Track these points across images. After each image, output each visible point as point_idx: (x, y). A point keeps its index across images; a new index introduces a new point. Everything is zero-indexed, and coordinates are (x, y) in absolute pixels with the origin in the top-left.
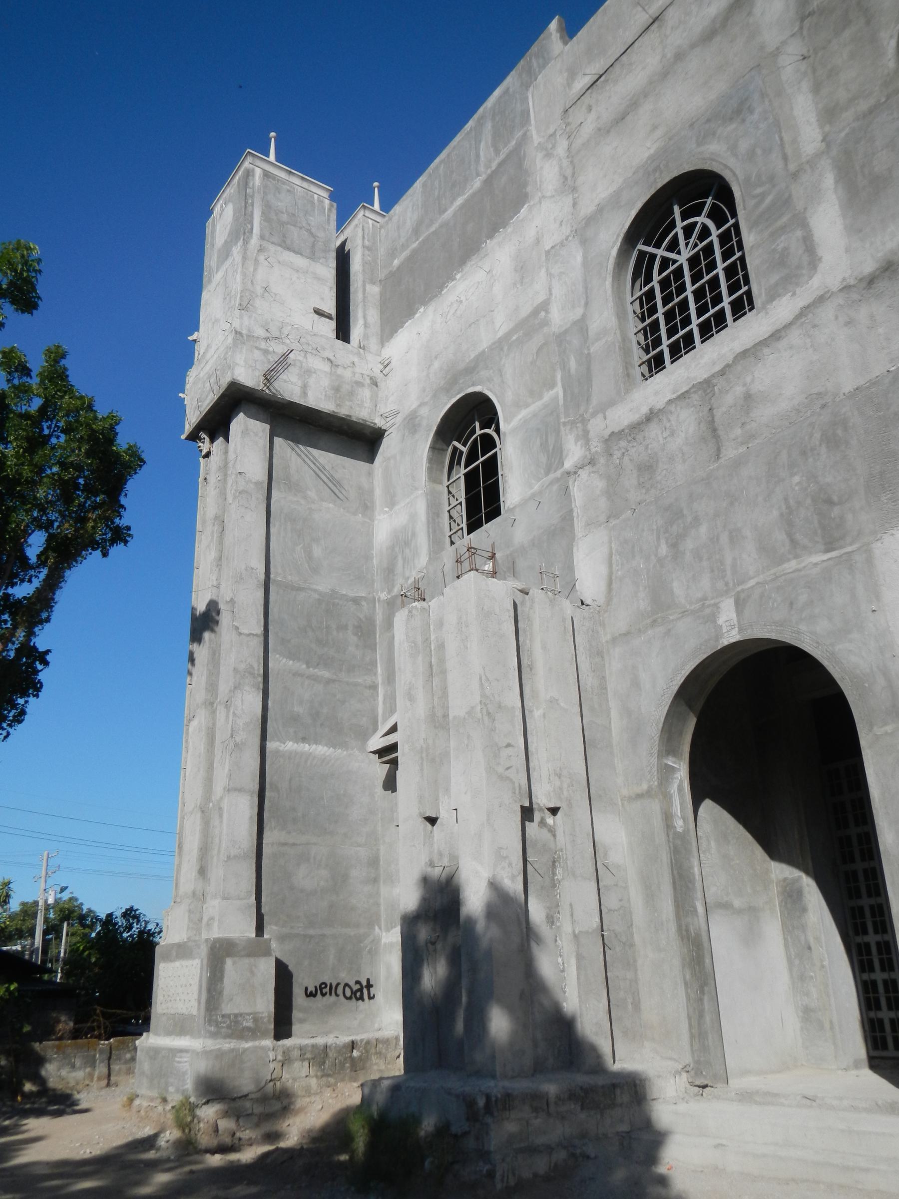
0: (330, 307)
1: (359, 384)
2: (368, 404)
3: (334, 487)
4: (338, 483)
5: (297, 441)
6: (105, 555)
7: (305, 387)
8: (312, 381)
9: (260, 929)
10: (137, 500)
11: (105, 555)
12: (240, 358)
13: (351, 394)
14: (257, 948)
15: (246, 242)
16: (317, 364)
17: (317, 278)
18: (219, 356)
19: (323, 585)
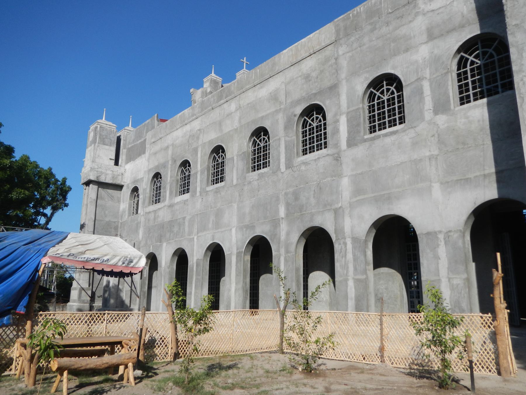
0: (113, 157)
1: (119, 175)
2: (120, 180)
3: (112, 197)
4: (113, 197)
5: (104, 188)
6: (63, 210)
7: (106, 178)
8: (107, 177)
10: (70, 197)
11: (63, 210)
12: (91, 174)
13: (116, 178)
15: (95, 145)
16: (109, 172)
19: (107, 219)
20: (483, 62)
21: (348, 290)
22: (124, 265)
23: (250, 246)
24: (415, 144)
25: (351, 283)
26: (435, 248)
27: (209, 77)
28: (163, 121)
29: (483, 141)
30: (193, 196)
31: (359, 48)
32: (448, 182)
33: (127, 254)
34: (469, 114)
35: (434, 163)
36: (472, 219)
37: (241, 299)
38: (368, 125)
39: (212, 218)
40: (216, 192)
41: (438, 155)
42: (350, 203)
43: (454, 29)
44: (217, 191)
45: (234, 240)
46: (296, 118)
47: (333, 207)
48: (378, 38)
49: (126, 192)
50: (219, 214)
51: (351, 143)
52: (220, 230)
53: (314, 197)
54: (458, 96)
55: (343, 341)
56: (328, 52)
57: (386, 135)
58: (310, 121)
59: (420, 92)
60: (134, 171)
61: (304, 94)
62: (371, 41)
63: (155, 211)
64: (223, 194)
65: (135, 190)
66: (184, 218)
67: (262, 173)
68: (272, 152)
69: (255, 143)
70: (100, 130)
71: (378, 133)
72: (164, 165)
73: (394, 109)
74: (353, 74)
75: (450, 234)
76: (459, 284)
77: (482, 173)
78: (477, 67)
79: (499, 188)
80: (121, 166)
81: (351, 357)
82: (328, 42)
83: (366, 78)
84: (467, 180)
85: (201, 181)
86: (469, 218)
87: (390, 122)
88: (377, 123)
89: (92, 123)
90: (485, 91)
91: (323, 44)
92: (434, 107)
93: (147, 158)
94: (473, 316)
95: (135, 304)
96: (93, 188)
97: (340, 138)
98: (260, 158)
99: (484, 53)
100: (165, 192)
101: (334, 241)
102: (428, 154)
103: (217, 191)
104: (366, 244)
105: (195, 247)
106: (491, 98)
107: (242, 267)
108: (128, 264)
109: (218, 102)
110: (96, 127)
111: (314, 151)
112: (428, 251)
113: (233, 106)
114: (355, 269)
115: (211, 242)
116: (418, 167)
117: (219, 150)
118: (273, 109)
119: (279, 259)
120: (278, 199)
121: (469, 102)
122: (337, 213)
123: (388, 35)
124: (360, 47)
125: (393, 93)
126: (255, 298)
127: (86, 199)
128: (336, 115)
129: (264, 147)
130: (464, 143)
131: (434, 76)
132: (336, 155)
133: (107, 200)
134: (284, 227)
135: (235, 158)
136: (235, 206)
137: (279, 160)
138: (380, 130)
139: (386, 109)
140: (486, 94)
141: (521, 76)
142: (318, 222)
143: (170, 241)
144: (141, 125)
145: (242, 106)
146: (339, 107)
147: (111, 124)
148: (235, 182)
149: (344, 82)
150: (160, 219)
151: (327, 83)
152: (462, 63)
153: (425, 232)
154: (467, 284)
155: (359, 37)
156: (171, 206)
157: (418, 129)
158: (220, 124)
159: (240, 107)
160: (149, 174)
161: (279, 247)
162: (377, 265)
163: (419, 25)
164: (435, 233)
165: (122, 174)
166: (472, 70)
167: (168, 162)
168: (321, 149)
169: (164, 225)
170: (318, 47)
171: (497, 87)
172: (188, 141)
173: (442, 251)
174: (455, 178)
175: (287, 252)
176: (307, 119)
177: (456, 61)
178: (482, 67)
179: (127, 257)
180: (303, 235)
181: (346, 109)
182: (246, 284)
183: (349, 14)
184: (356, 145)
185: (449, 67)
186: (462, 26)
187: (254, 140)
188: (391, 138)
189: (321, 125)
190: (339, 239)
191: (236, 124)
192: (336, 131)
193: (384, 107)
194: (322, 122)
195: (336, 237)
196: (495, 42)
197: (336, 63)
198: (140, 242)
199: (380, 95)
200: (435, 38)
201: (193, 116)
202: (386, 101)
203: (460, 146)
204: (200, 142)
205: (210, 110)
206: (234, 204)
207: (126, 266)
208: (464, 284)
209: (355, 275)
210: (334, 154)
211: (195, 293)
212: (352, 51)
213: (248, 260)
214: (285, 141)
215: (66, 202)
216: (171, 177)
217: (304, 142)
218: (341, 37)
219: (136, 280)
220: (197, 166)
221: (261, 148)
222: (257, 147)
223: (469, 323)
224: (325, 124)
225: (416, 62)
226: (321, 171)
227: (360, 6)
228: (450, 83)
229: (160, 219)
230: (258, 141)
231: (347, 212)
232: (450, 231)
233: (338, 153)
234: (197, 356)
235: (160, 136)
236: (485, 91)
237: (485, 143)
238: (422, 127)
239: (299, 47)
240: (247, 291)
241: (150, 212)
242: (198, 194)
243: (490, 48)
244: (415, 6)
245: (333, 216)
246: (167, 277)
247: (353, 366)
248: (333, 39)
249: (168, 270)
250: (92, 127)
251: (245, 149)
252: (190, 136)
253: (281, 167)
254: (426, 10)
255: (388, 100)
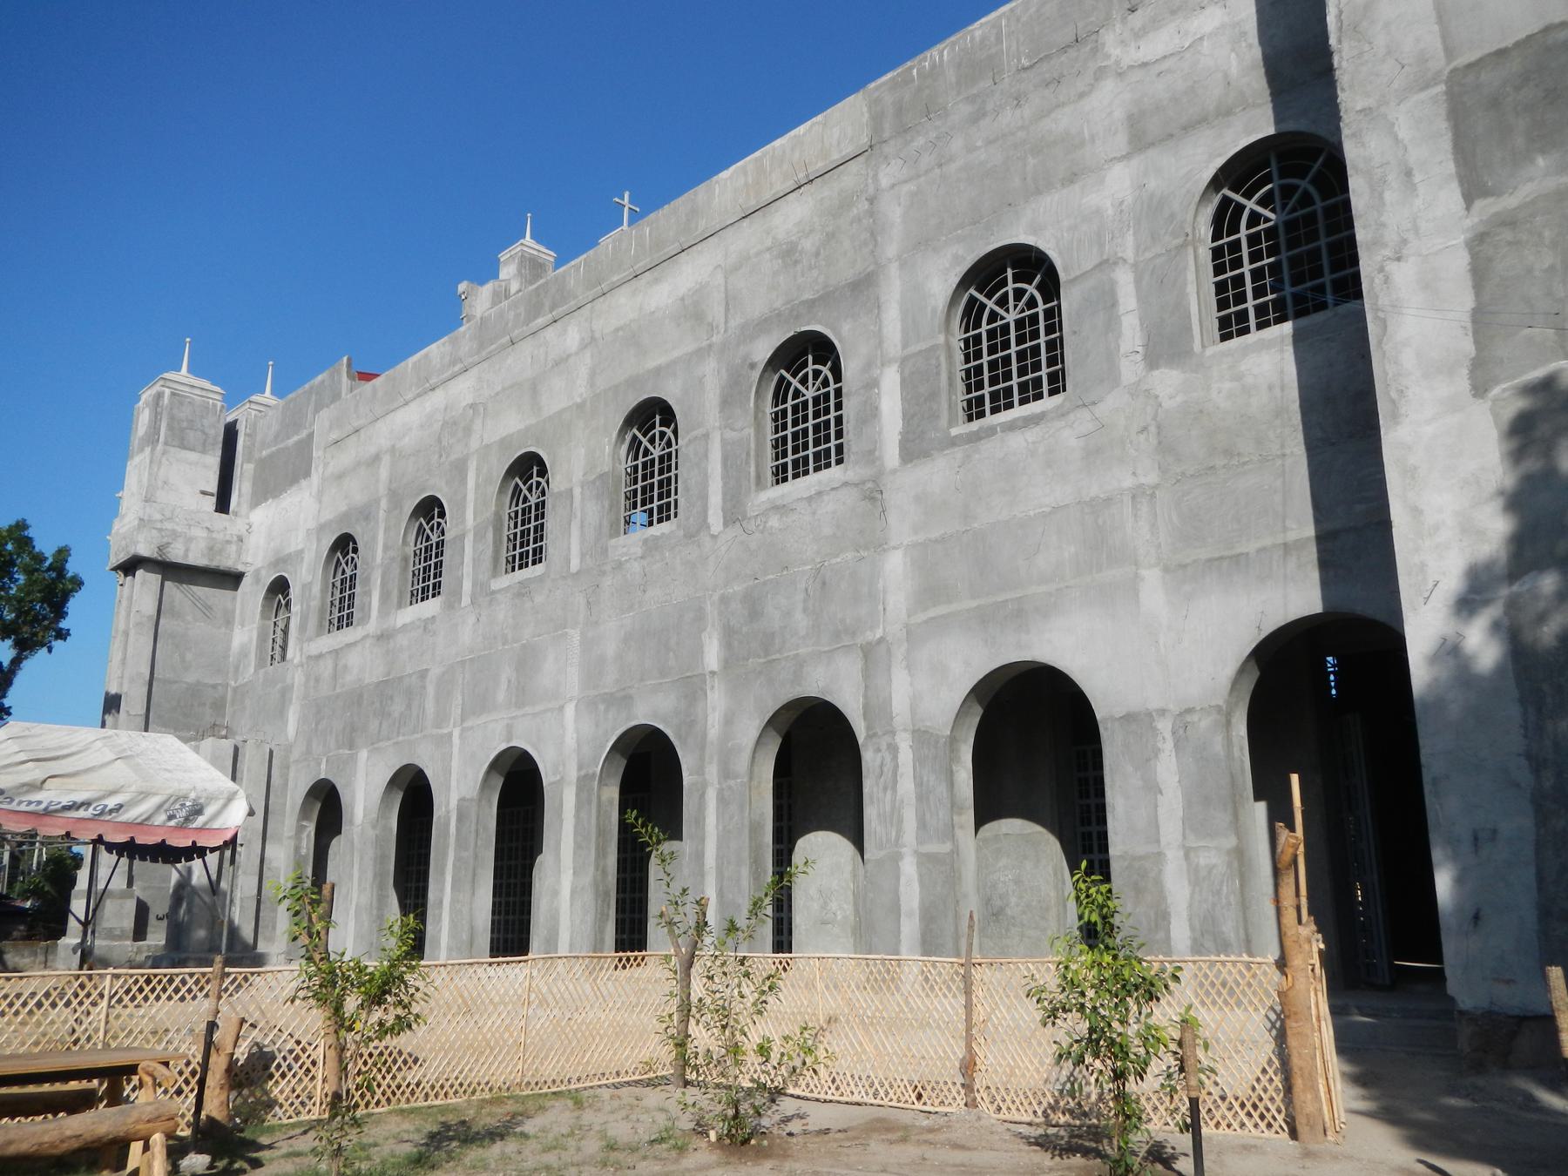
0: (213, 486)
1: (228, 542)
2: (234, 555)
3: (207, 610)
4: (210, 608)
5: (181, 582)
6: (50, 651)
7: (187, 550)
8: (193, 546)
9: (130, 883)
11: (50, 651)
12: (141, 538)
13: (221, 551)
14: (123, 895)
15: (153, 450)
16: (199, 533)
17: (205, 466)
18: (130, 531)
19: (191, 678)
20: (1284, 217)
21: (902, 889)
22: (172, 823)
23: (618, 757)
24: (1095, 453)
25: (909, 868)
26: (1148, 760)
27: (516, 249)
28: (366, 377)
29: (1283, 446)
30: (450, 606)
31: (937, 171)
32: (1183, 566)
33: (185, 787)
34: (1243, 368)
35: (1144, 508)
36: (1254, 675)
37: (590, 918)
38: (960, 396)
39: (507, 673)
40: (520, 595)
41: (1156, 486)
42: (907, 626)
43: (1202, 121)
44: (523, 591)
45: (570, 740)
46: (756, 374)
47: (860, 640)
48: (989, 142)
49: (251, 594)
50: (527, 661)
51: (914, 449)
52: (528, 709)
53: (805, 610)
54: (1213, 315)
55: (861, 1044)
56: (849, 178)
57: (1011, 427)
58: (795, 383)
59: (1107, 300)
60: (277, 530)
61: (778, 304)
62: (971, 149)
63: (336, 653)
64: (539, 599)
65: (280, 587)
66: (423, 674)
67: (656, 538)
68: (685, 474)
69: (635, 445)
70: (171, 403)
71: (990, 420)
72: (366, 513)
73: (1036, 350)
74: (922, 243)
75: (1188, 718)
76: (1214, 866)
77: (1280, 540)
78: (1266, 230)
79: (1325, 584)
80: (236, 514)
81: (882, 1093)
82: (849, 150)
83: (957, 259)
84: (1238, 560)
85: (476, 562)
86: (1242, 671)
87: (1023, 387)
88: (987, 390)
89: (148, 378)
90: (1289, 301)
91: (836, 157)
92: (1146, 346)
93: (315, 490)
94: (1223, 963)
95: (271, 940)
96: (146, 580)
97: (880, 433)
98: (651, 488)
99: (1287, 191)
100: (368, 593)
101: (860, 741)
102: (1129, 482)
103: (523, 591)
104: (952, 751)
105: (455, 764)
106: (1304, 321)
107: (594, 821)
108: (187, 819)
109: (528, 321)
110: (159, 395)
111: (806, 473)
112: (1130, 769)
113: (571, 335)
114: (922, 824)
115: (504, 746)
116: (1100, 521)
117: (528, 467)
118: (689, 347)
119: (702, 796)
120: (700, 617)
121: (1245, 331)
122: (872, 657)
123: (1020, 134)
124: (940, 165)
125: (1032, 303)
126: (637, 916)
127: (123, 613)
128: (868, 366)
129: (661, 458)
130: (1228, 453)
131: (1148, 255)
132: (870, 485)
133: (189, 618)
134: (716, 701)
135: (577, 491)
136: (575, 635)
137: (704, 497)
138: (995, 410)
139: (1013, 349)
140: (1290, 310)
141: (1379, 258)
142: (815, 684)
143: (381, 744)
144: (300, 391)
145: (597, 335)
146: (880, 343)
147: (207, 384)
148: (575, 564)
149: (894, 270)
150: (349, 678)
151: (846, 272)
152: (1225, 219)
153: (1119, 712)
154: (1236, 864)
155: (938, 138)
156: (383, 637)
157: (1102, 410)
158: (534, 388)
159: (593, 339)
160: (319, 540)
161: (702, 758)
162: (987, 809)
163: (1106, 104)
164: (1149, 714)
165: (241, 540)
166: (1253, 240)
167: (377, 501)
168: (828, 466)
169: (361, 696)
170: (820, 164)
171: (1321, 289)
172: (439, 441)
173: (1168, 769)
174: (1204, 554)
175: (726, 774)
176: (788, 376)
177: (1209, 211)
178: (1281, 230)
179: (185, 797)
180: (772, 722)
181: (899, 347)
182: (604, 872)
183: (911, 68)
184: (926, 454)
185: (1189, 230)
186: (1225, 112)
187: (635, 437)
188: (1028, 434)
189: (827, 395)
190: (875, 735)
191: (581, 391)
192: (871, 413)
193: (1006, 345)
194: (832, 387)
195: (868, 728)
196: (1315, 161)
197: (871, 214)
198: (289, 749)
199: (997, 309)
200: (1153, 144)
201: (453, 363)
202: (1013, 324)
203: (1219, 462)
204: (475, 443)
205: (504, 348)
206: (570, 631)
207: (180, 827)
208: (1229, 865)
209: (920, 841)
210: (864, 483)
211: (453, 901)
212: (919, 176)
213: (611, 802)
214: (724, 442)
215: (63, 624)
216: (386, 548)
217: (779, 445)
218: (886, 135)
219: (275, 864)
220: (464, 513)
221: (653, 461)
222: (641, 460)
223: (1213, 984)
224: (838, 392)
225: (1098, 212)
226: (827, 531)
227: (940, 46)
228: (1191, 276)
229: (349, 678)
230: (645, 442)
231: (899, 653)
232: (1189, 711)
233: (875, 480)
234: (408, 1100)
235: (356, 424)
236: (1289, 301)
237: (1288, 451)
238: (1112, 404)
239: (767, 162)
240: (607, 894)
241: (320, 656)
242: (466, 600)
243: (1303, 178)
244: (1095, 51)
245: (859, 665)
246: (370, 853)
247: (879, 1120)
248: (865, 140)
249: (371, 833)
250: (147, 395)
251: (605, 465)
252: (445, 424)
253: (711, 520)
254: (1126, 61)
255: (1020, 324)
